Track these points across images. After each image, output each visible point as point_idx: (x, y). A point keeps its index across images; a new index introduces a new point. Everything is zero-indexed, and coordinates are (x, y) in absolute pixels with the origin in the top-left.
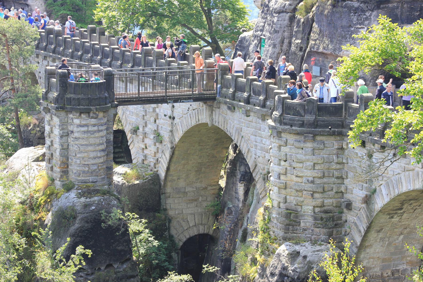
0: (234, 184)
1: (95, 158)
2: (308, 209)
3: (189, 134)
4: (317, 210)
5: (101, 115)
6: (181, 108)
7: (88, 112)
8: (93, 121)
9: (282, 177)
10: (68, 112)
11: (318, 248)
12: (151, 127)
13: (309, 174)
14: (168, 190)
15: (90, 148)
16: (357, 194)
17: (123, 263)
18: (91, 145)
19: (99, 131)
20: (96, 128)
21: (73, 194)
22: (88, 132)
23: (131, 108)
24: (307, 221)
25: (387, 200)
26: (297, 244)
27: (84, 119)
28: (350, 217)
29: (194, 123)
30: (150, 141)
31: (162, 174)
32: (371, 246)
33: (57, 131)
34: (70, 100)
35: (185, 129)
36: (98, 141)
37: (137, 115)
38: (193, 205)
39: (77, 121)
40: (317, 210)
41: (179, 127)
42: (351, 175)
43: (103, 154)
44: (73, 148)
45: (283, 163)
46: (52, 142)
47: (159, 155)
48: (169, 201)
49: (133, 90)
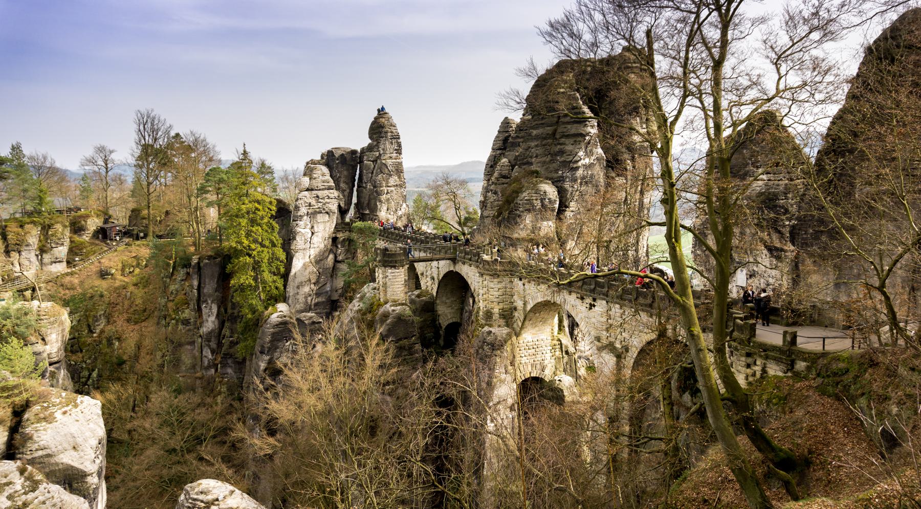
3: (446, 275)
6: (442, 263)
7: (395, 267)
10: (385, 267)
12: (429, 272)
13: (496, 294)
16: (519, 304)
21: (388, 306)
23: (421, 263)
24: (496, 316)
25: (532, 305)
27: (394, 270)
28: (516, 314)
30: (428, 279)
31: (435, 294)
33: (381, 276)
44: (389, 283)
49: (422, 254)
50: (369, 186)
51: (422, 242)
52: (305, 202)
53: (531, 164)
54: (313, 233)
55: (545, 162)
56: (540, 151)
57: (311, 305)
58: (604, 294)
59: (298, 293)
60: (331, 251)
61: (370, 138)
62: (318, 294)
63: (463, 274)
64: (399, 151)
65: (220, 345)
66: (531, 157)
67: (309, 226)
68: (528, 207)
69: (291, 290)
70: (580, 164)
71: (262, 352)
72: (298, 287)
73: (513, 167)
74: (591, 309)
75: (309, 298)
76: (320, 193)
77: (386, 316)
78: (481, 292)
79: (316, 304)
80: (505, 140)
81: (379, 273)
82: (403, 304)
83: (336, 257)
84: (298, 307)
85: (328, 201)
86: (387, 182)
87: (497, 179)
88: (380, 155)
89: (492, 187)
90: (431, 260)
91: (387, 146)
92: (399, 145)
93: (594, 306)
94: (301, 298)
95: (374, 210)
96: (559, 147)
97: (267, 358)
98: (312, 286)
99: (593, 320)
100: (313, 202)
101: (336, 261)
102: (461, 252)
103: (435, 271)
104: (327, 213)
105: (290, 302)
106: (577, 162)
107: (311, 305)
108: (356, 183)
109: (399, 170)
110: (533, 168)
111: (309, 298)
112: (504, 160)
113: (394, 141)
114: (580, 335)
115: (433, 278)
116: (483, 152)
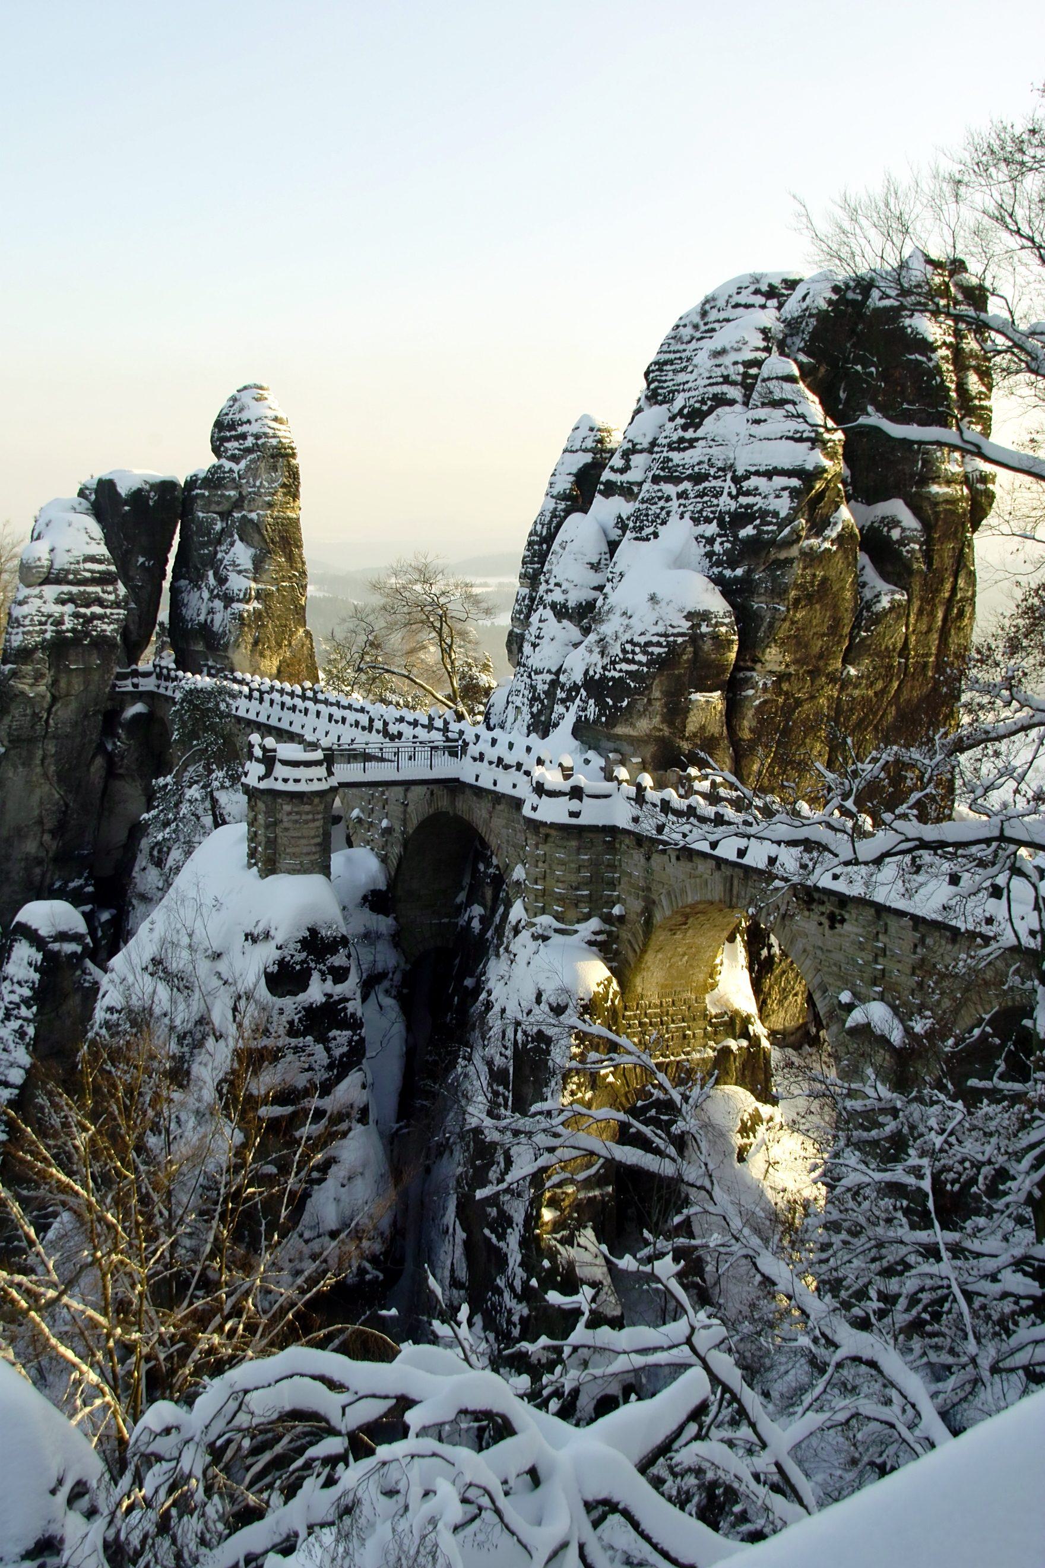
1: (308, 854)
3: (423, 825)
8: (307, 808)
15: (303, 841)
19: (314, 820)
20: (310, 817)
29: (431, 811)
36: (312, 833)
39: (287, 808)
41: (414, 816)
42: (624, 880)
43: (318, 849)
44: (282, 840)
45: (540, 864)
54: (55, 699)
61: (217, 451)
64: (292, 489)
67: (48, 680)
70: (794, 551)
74: (832, 927)
93: (843, 921)
98: (47, 837)
99: (838, 956)
101: (111, 772)
106: (788, 543)
108: (169, 568)
111: (38, 870)
114: (775, 995)
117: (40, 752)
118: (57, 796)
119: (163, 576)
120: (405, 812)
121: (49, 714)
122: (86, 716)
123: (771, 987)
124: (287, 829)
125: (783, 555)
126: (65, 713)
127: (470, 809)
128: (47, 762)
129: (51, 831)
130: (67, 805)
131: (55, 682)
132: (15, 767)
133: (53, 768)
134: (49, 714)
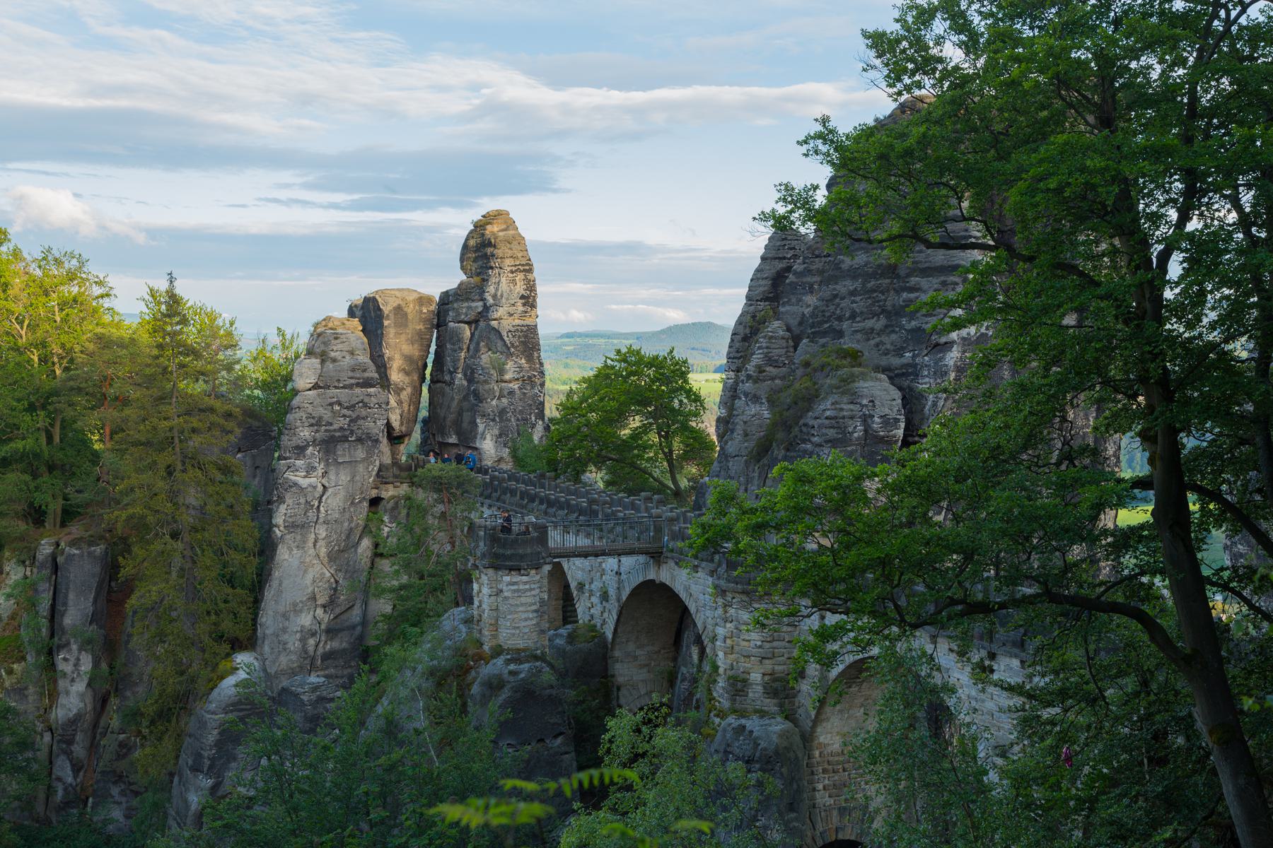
0: (688, 647)
1: (526, 620)
2: (756, 677)
4: (767, 678)
5: (533, 572)
6: (628, 561)
8: (525, 578)
9: (728, 641)
11: (767, 722)
12: (596, 585)
14: (617, 653)
15: (521, 609)
17: (556, 737)
18: (522, 605)
19: (531, 590)
21: (500, 661)
22: (518, 591)
23: (578, 562)
24: (756, 693)
26: (743, 717)
30: (595, 600)
31: (610, 636)
32: (828, 719)
33: (485, 590)
34: (496, 556)
35: (634, 585)
36: (529, 600)
37: (583, 570)
38: (645, 670)
40: (767, 678)
41: (626, 584)
46: (480, 602)
47: (606, 615)
48: (618, 666)
50: (459, 378)
51: (581, 512)
52: (310, 416)
53: (840, 334)
55: (872, 329)
56: (860, 304)
57: (313, 658)
58: (1014, 644)
59: (284, 630)
60: (366, 530)
62: (331, 632)
63: (678, 588)
64: (529, 300)
65: (93, 746)
66: (840, 319)
67: (320, 472)
68: (831, 433)
69: (268, 620)
70: (954, 335)
71: (196, 769)
72: (285, 616)
73: (797, 340)
75: (312, 642)
76: (343, 395)
77: (494, 686)
78: (721, 631)
79: (327, 656)
80: (778, 280)
81: (483, 588)
82: (536, 658)
83: (376, 545)
84: (284, 661)
85: (364, 412)
86: (502, 371)
87: (760, 370)
88: (486, 308)
89: (748, 386)
90: (604, 554)
91: (504, 285)
92: (531, 287)
93: (992, 671)
94: (294, 643)
95: (468, 438)
96: (905, 295)
97: (210, 782)
98: (320, 612)
100: (327, 415)
101: (377, 554)
102: (674, 537)
103: (610, 580)
104: (359, 440)
105: (266, 648)
107: (313, 658)
109: (528, 342)
110: (848, 343)
111: (312, 642)
112: (776, 326)
113: (520, 276)
115: (605, 597)
116: (726, 305)
117: (313, 536)
118: (328, 575)
119: (423, 379)
120: (620, 582)
121: (320, 502)
122: (352, 503)
123: (952, 735)
124: (506, 598)
125: (943, 340)
126: (334, 502)
127: (673, 578)
128: (318, 545)
129: (324, 606)
130: (337, 582)
131: (325, 474)
132: (290, 549)
133: (323, 551)
134: (320, 502)
